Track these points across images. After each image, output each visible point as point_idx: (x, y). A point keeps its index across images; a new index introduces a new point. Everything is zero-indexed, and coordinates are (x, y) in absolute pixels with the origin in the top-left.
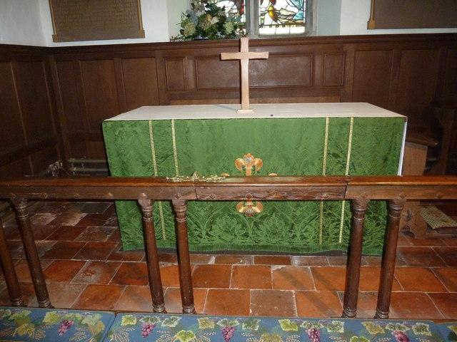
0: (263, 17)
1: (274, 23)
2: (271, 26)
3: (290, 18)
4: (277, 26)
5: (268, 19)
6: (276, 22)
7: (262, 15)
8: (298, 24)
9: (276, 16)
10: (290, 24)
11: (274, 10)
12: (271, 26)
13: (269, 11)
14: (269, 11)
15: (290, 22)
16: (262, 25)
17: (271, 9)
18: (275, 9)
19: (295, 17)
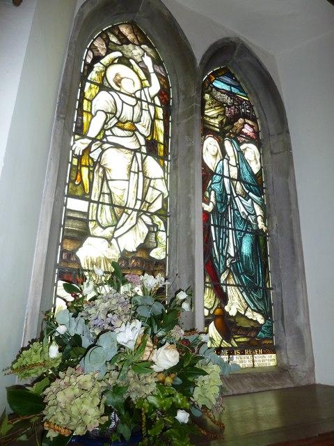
1: (225, 344)
3: (252, 335)
6: (228, 341)
11: (225, 315)
17: (218, 311)
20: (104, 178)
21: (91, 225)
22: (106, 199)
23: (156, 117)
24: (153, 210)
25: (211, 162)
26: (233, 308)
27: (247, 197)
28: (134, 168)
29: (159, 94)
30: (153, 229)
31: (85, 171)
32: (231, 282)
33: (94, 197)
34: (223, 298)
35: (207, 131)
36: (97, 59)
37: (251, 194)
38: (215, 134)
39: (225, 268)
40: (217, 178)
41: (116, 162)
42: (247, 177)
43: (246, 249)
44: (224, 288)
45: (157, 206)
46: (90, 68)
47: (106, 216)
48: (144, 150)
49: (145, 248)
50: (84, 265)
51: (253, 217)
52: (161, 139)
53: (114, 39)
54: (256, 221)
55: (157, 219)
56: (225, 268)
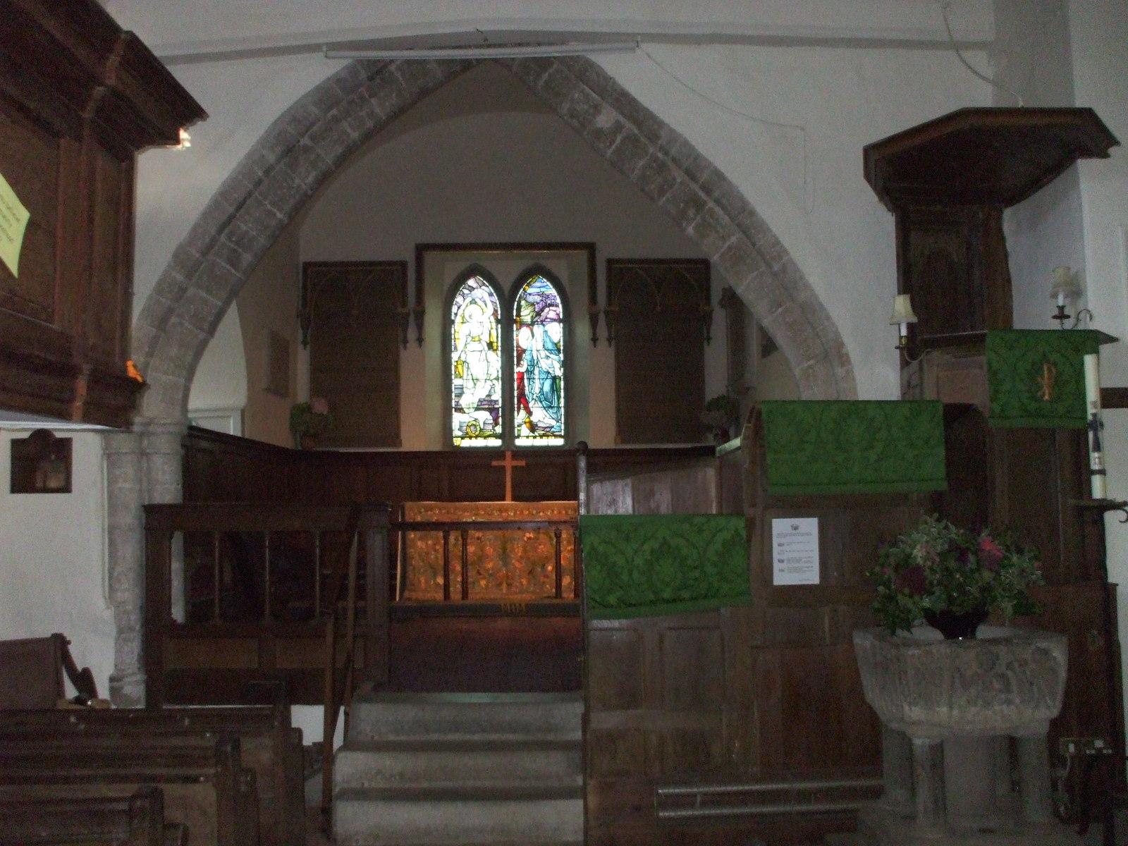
0: (519, 428)
1: (532, 434)
2: (528, 437)
4: (535, 437)
5: (525, 430)
6: (533, 433)
7: (518, 426)
8: (556, 436)
9: (533, 427)
10: (548, 436)
11: (531, 422)
12: (528, 437)
13: (525, 423)
14: (525, 423)
15: (548, 433)
16: (518, 436)
17: (527, 420)
18: (532, 421)
19: (553, 430)
20: (468, 368)
21: (465, 390)
22: (470, 377)
23: (492, 328)
24: (492, 378)
25: (523, 345)
26: (534, 419)
27: (547, 357)
28: (482, 360)
29: (493, 314)
30: (493, 387)
31: (460, 367)
32: (536, 405)
33: (465, 378)
34: (530, 413)
35: (522, 324)
36: (459, 308)
37: (552, 356)
38: (528, 325)
39: (533, 399)
40: (528, 353)
41: (473, 359)
42: (550, 346)
43: (547, 387)
44: (531, 409)
45: (494, 375)
46: (456, 314)
47: (471, 384)
48: (486, 348)
49: (489, 396)
50: (463, 407)
51: (553, 369)
52: (495, 340)
53: (466, 291)
54: (554, 371)
55: (495, 382)
56: (533, 399)
